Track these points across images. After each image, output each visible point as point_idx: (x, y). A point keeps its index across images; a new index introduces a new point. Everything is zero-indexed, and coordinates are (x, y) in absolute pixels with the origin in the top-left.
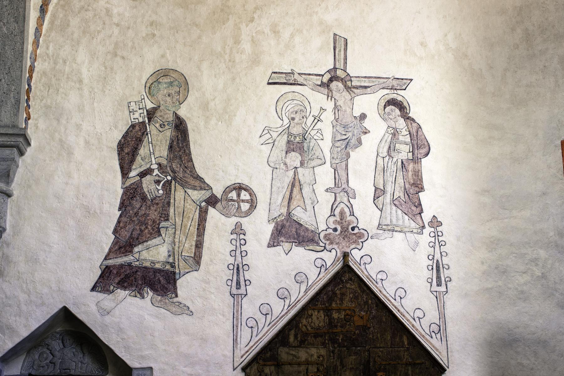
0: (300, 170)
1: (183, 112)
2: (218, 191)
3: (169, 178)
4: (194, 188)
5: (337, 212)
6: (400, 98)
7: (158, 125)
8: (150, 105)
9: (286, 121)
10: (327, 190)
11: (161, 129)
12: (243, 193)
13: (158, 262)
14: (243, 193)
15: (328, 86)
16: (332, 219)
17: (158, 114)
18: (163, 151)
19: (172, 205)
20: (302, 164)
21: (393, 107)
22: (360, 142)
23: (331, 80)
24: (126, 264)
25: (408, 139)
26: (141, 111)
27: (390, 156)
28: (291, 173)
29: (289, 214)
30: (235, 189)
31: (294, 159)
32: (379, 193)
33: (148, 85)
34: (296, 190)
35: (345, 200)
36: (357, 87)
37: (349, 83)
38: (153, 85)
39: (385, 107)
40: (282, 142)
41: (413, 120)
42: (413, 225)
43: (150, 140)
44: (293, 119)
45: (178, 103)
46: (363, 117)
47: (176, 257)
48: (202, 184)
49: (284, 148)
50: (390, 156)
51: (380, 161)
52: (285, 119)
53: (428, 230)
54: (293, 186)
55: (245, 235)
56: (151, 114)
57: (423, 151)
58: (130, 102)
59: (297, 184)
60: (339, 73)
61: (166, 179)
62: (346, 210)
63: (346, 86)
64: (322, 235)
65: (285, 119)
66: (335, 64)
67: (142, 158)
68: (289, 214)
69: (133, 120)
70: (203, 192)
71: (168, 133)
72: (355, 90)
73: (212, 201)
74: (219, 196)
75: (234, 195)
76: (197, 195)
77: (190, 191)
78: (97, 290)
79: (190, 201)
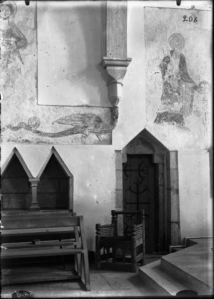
1: (183, 52)
8: (171, 49)
17: (174, 52)
18: (177, 67)
48: (192, 82)
56: (172, 52)
71: (178, 60)
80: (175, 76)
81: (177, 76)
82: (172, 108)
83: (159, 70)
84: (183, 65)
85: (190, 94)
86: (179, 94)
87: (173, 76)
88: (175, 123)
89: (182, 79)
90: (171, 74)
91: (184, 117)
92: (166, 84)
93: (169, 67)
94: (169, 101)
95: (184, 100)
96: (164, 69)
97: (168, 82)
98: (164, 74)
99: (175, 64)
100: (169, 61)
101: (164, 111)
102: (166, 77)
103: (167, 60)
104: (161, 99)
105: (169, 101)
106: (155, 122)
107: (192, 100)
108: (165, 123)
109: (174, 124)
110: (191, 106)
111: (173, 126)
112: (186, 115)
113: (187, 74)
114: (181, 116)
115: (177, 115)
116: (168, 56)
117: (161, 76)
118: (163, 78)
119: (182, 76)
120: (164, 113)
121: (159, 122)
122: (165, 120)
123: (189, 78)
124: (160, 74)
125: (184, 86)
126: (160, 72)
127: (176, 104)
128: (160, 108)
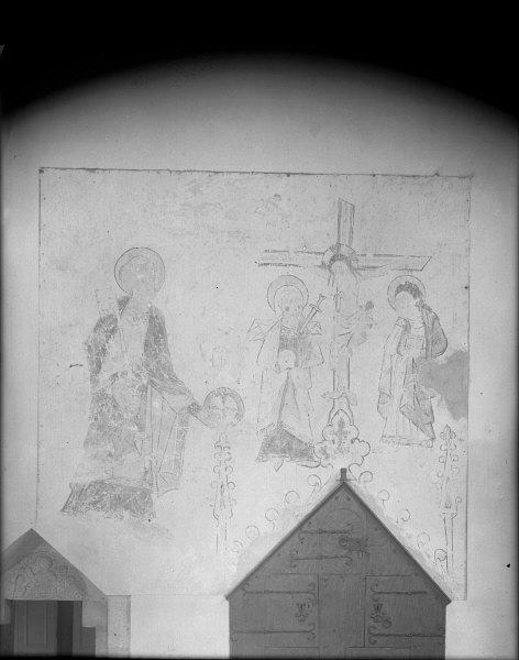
0: (294, 373)
3: (145, 382)
5: (336, 420)
6: (416, 282)
7: (130, 318)
8: (121, 294)
9: (279, 311)
10: (324, 396)
12: (229, 399)
14: (229, 399)
15: (330, 267)
16: (328, 430)
17: (130, 304)
18: (137, 349)
20: (296, 364)
21: (406, 293)
22: (364, 335)
23: (333, 260)
25: (422, 332)
27: (399, 353)
28: (284, 375)
29: (280, 424)
31: (289, 356)
32: (384, 396)
33: (120, 265)
34: (289, 396)
35: (345, 408)
36: (364, 268)
37: (354, 264)
39: (397, 292)
40: (273, 340)
41: (429, 309)
42: (422, 436)
44: (287, 309)
46: (370, 305)
49: (276, 342)
50: (399, 353)
51: (388, 361)
52: (278, 309)
53: (439, 441)
54: (285, 390)
56: (123, 303)
57: (440, 347)
59: (290, 389)
60: (344, 250)
62: (346, 419)
63: (350, 266)
64: (317, 448)
65: (278, 309)
66: (339, 239)
68: (280, 424)
70: (183, 398)
71: (143, 327)
72: (362, 272)
73: (194, 409)
75: (218, 400)
80: (130, 376)
81: (137, 375)
83: (82, 357)
84: (157, 341)
85: (177, 427)
86: (142, 428)
88: (126, 514)
91: (154, 496)
92: (100, 397)
93: (113, 347)
95: (155, 445)
96: (97, 355)
97: (109, 392)
98: (97, 367)
99: (133, 332)
100: (113, 331)
101: (92, 479)
102: (104, 376)
103: (107, 325)
104: (86, 443)
108: (93, 513)
113: (170, 370)
114: (145, 494)
115: (133, 490)
117: (88, 374)
118: (94, 381)
123: (174, 380)
124: (86, 370)
125: (156, 404)
126: (86, 364)
127: (131, 457)
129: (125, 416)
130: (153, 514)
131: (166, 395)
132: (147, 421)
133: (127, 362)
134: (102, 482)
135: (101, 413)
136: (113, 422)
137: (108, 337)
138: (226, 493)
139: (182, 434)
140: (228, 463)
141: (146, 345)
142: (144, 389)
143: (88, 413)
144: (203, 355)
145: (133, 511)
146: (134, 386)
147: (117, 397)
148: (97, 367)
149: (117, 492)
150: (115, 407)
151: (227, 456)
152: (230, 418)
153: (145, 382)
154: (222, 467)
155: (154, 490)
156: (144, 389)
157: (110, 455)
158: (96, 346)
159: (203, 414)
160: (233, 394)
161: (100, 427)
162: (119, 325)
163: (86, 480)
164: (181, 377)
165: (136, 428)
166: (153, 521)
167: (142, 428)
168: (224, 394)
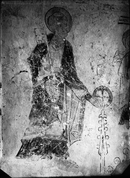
2: (91, 91)
4: (77, 88)
7: (54, 46)
8: (48, 32)
11: (56, 49)
12: (105, 92)
13: (58, 136)
14: (105, 92)
17: (54, 38)
18: (58, 63)
19: (64, 99)
24: (38, 138)
26: (43, 36)
30: (100, 89)
33: (47, 18)
38: (50, 18)
43: (50, 56)
45: (66, 32)
47: (68, 132)
48: (83, 88)
55: (106, 118)
58: (36, 29)
61: (60, 83)
67: (45, 68)
69: (38, 42)
70: (82, 91)
73: (88, 97)
74: (91, 93)
75: (99, 93)
76: (81, 93)
77: (75, 90)
78: (20, 156)
79: (75, 97)
80: (54, 78)
81: (58, 78)
82: (50, 132)
83: (27, 67)
85: (80, 107)
86: (61, 108)
87: (51, 77)
88: (53, 155)
89: (66, 82)
90: (47, 74)
91: (68, 145)
93: (45, 62)
94: (43, 119)
95: (69, 117)
97: (43, 87)
98: (35, 74)
100: (45, 53)
101: (35, 136)
102: (40, 78)
104: (30, 116)
105: (43, 119)
106: (17, 155)
107: (82, 118)
108: (35, 156)
109: (51, 158)
110: (80, 127)
111: (50, 161)
112: (72, 141)
113: (75, 75)
114: (64, 144)
115: (57, 142)
116: (43, 44)
118: (34, 81)
119: (66, 78)
120: (34, 140)
121: (25, 155)
122: (35, 151)
123: (78, 81)
125: (69, 94)
126: (29, 70)
127: (56, 124)
128: (27, 132)
129: (52, 101)
130: (68, 155)
131: (73, 89)
132: (64, 103)
133: (53, 71)
134: (39, 139)
135: (39, 99)
136: (45, 104)
137: (42, 56)
138: (104, 142)
139: (83, 111)
140: (106, 126)
141: (63, 62)
142: (61, 86)
143: (31, 99)
144: (92, 68)
145: (57, 154)
146: (56, 84)
147: (48, 90)
148: (35, 74)
149: (49, 144)
150: (46, 96)
151: (105, 122)
152: (106, 101)
153: (62, 82)
154: (103, 128)
155: (68, 141)
156: (61, 86)
157: (44, 122)
158: (35, 61)
159: (92, 100)
160: (107, 90)
161: (39, 107)
162: (48, 49)
163: (30, 137)
164: (81, 80)
165: (58, 108)
166: (68, 159)
167: (61, 108)
168: (102, 89)
